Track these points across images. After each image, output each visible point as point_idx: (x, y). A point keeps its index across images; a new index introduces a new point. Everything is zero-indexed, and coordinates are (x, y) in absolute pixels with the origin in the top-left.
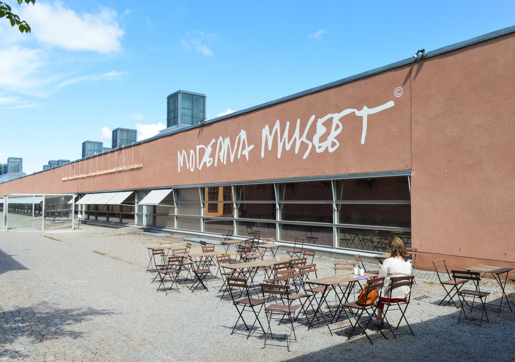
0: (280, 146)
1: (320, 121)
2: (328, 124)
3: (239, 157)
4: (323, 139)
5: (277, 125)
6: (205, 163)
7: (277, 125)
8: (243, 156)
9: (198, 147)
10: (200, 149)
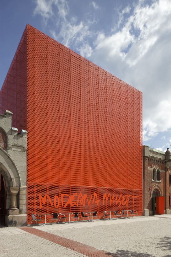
0: (111, 202)
1: (124, 197)
2: (125, 198)
3: (93, 203)
4: (124, 201)
5: (110, 194)
6: (69, 205)
7: (110, 194)
8: (95, 203)
9: (62, 195)
10: (64, 197)
